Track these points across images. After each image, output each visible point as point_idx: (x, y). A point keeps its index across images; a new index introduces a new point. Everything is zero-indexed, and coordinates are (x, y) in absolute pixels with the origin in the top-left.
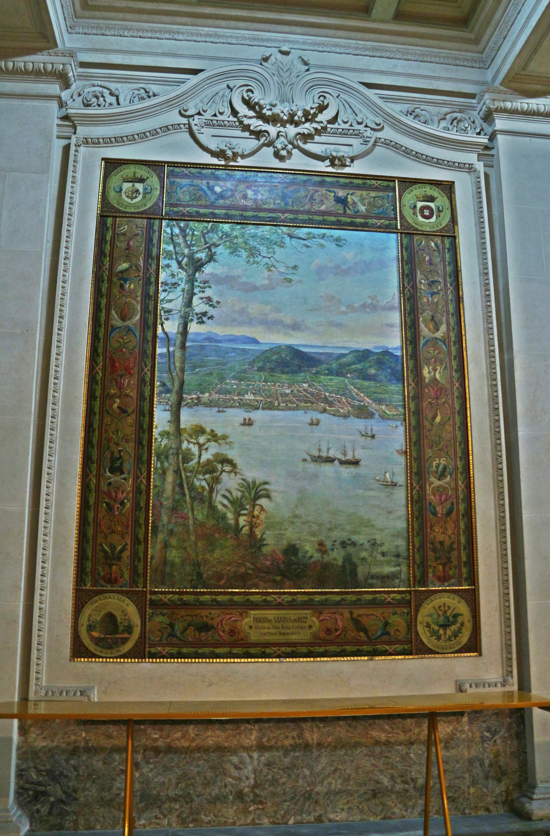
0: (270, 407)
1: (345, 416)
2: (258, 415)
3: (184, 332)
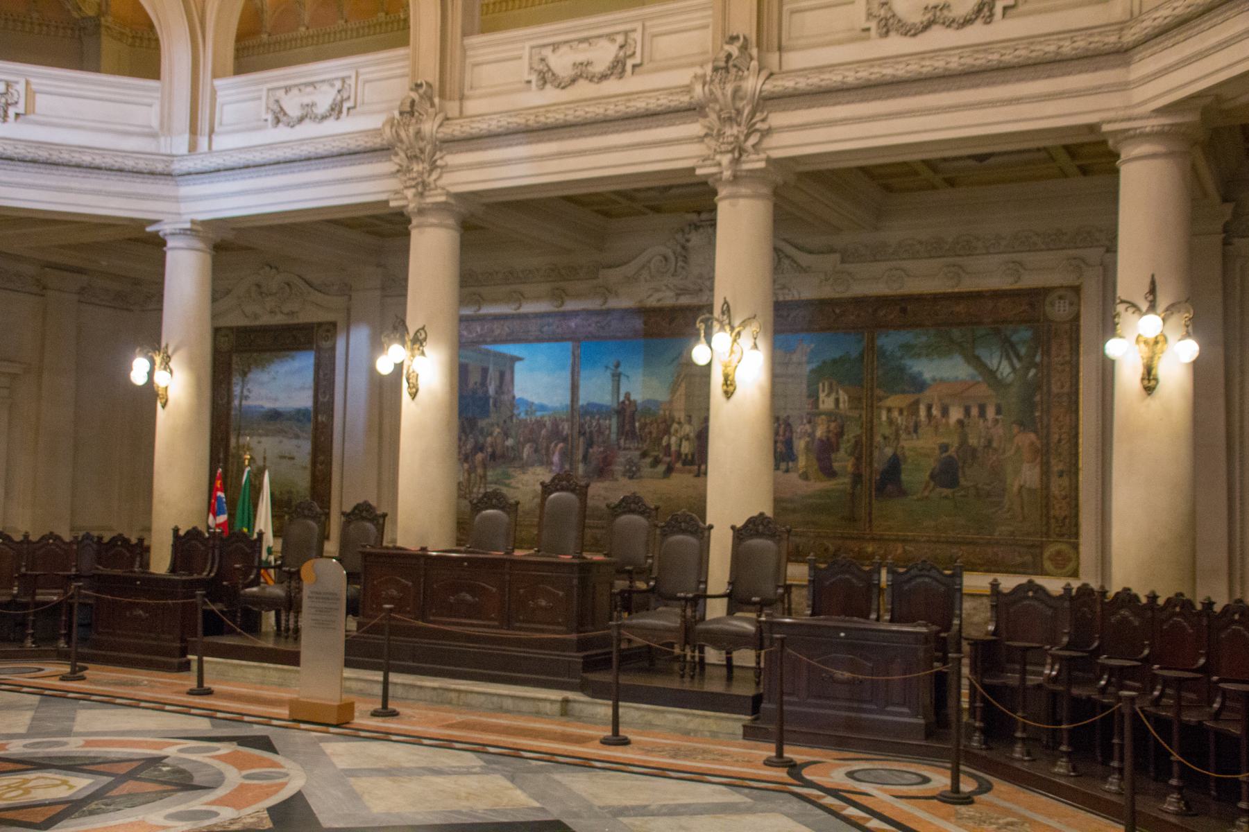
0: (267, 435)
1: (291, 438)
2: (264, 439)
3: (240, 405)
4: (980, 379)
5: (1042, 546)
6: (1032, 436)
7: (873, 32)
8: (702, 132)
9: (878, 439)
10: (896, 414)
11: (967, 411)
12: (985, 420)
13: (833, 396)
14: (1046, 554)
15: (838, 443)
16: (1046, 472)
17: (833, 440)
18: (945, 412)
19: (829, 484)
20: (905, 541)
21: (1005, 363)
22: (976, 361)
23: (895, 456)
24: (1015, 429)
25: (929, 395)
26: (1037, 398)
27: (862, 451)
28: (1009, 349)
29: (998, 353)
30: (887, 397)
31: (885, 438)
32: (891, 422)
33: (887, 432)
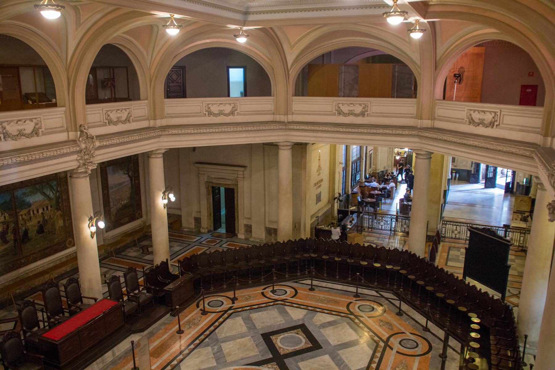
4: (46, 199)
5: (65, 241)
6: (60, 212)
7: (107, 124)
8: (79, 158)
9: (20, 225)
10: (24, 216)
11: (43, 209)
12: (48, 211)
13: (3, 216)
14: (67, 243)
15: (7, 231)
16: (64, 221)
17: (6, 231)
18: (38, 211)
19: (6, 246)
20: (33, 254)
21: (51, 193)
22: (44, 194)
23: (25, 229)
24: (56, 211)
25: (33, 207)
26: (60, 201)
27: (16, 231)
28: (51, 188)
29: (49, 190)
30: (20, 212)
31: (22, 225)
32: (23, 219)
33: (22, 222)
